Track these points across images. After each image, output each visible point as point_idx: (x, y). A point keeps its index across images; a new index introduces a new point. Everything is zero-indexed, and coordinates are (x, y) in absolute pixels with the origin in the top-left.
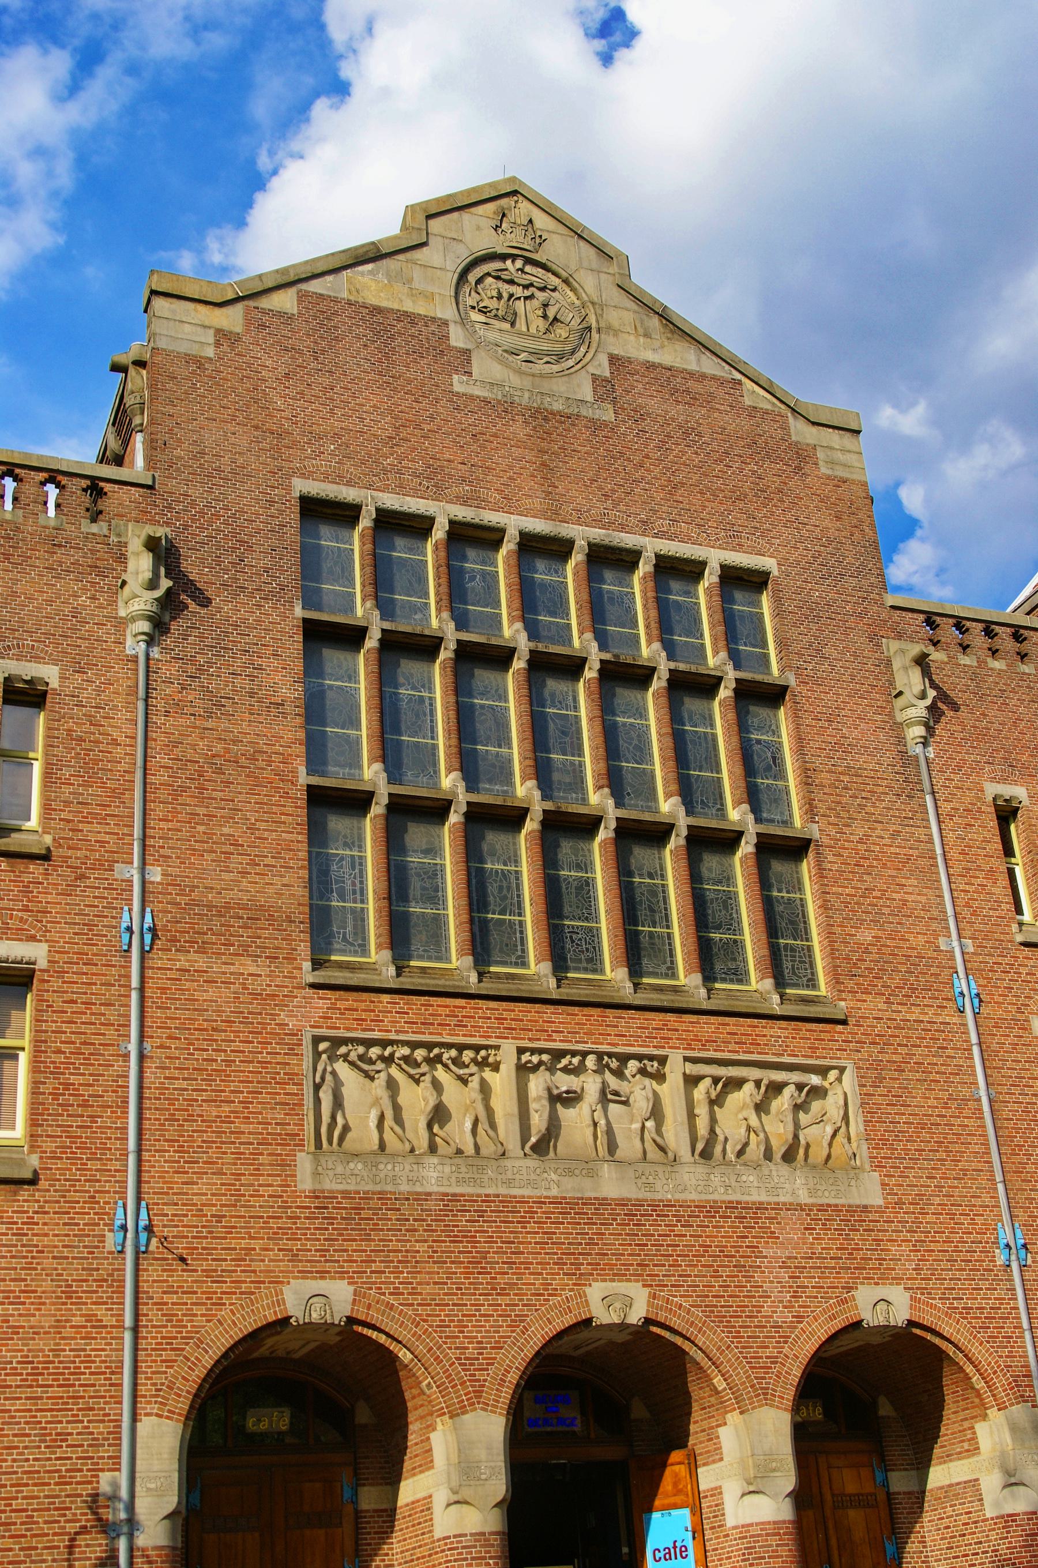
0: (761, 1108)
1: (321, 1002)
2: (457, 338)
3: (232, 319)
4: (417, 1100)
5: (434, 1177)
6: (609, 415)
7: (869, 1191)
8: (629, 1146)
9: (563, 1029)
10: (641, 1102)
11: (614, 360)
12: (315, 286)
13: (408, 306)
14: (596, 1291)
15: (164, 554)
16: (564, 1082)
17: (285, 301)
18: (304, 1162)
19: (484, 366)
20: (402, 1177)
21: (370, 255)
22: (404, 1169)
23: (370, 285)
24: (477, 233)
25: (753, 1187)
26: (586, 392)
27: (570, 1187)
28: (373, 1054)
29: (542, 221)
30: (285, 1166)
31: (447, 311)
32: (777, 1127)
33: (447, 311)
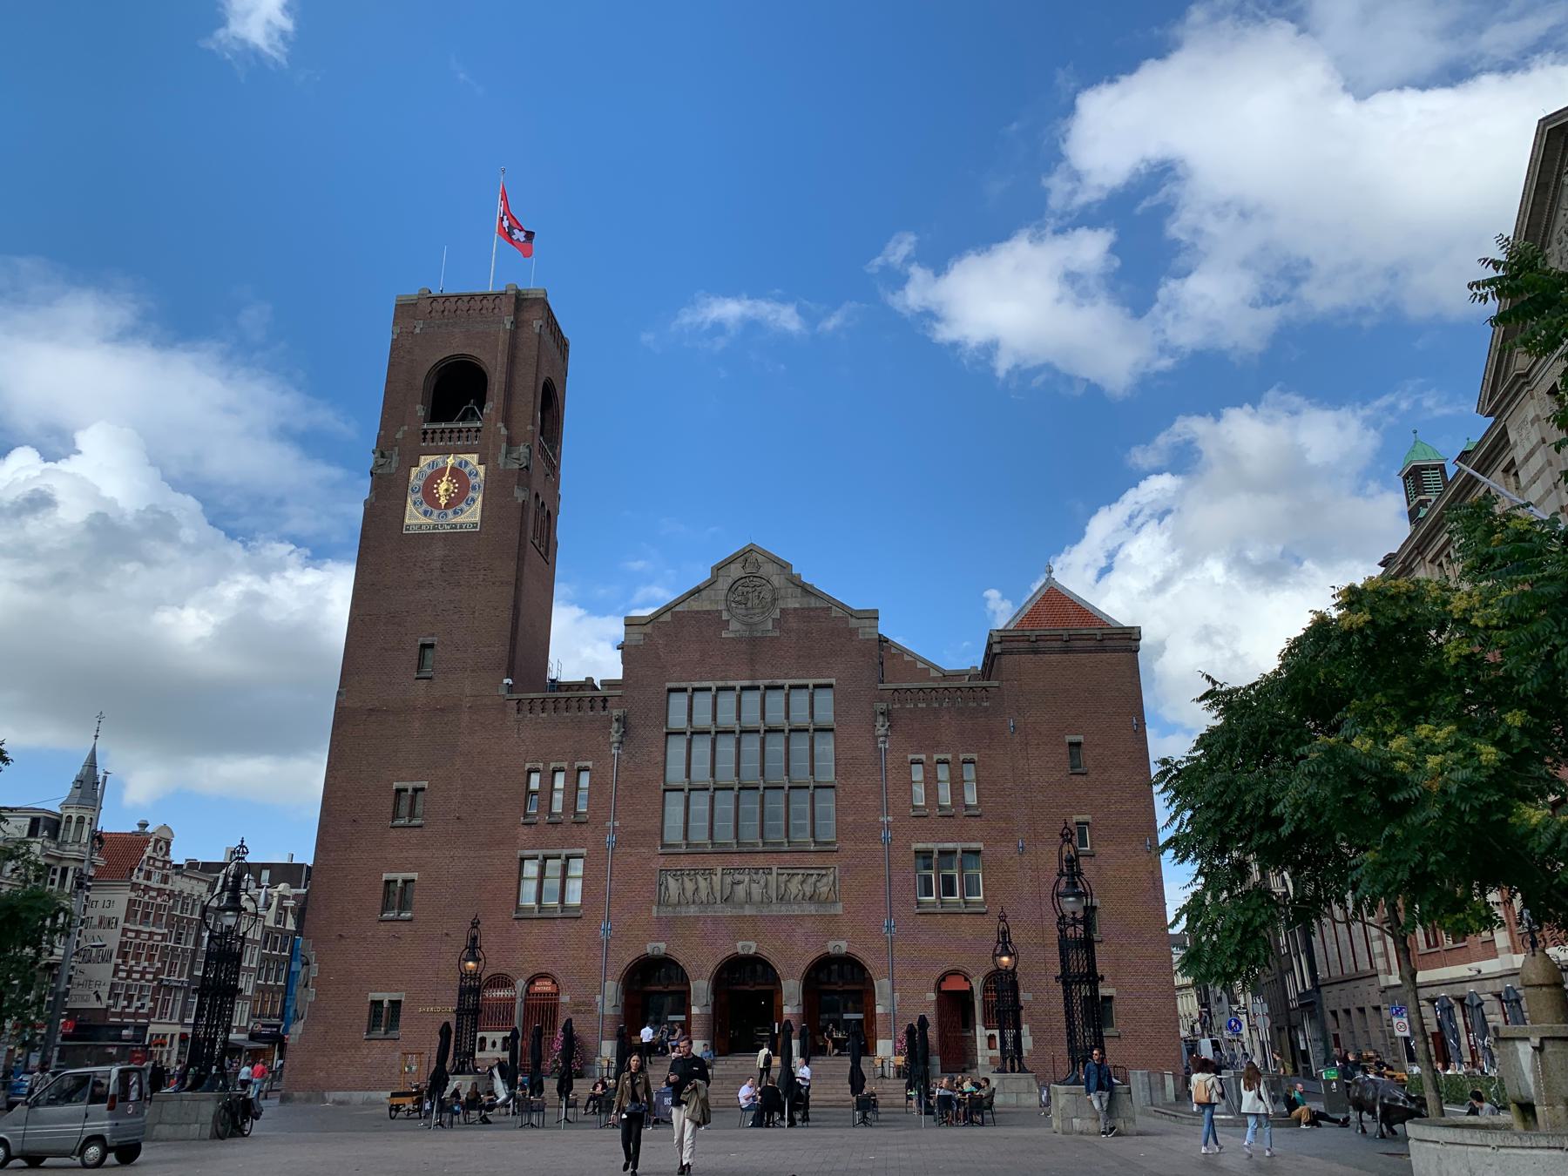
0: (803, 882)
1: (662, 859)
2: (725, 616)
3: (648, 629)
4: (689, 886)
5: (693, 910)
6: (777, 634)
7: (839, 909)
8: (756, 896)
9: (737, 861)
10: (762, 883)
11: (783, 611)
12: (677, 609)
13: (708, 608)
14: (740, 944)
15: (623, 721)
16: (738, 877)
17: (667, 617)
18: (655, 908)
19: (734, 625)
20: (684, 911)
21: (697, 591)
22: (684, 909)
23: (694, 605)
24: (736, 571)
25: (796, 910)
26: (770, 626)
27: (735, 912)
28: (678, 874)
29: (761, 559)
30: (650, 910)
31: (722, 607)
32: (808, 889)
33: (722, 607)
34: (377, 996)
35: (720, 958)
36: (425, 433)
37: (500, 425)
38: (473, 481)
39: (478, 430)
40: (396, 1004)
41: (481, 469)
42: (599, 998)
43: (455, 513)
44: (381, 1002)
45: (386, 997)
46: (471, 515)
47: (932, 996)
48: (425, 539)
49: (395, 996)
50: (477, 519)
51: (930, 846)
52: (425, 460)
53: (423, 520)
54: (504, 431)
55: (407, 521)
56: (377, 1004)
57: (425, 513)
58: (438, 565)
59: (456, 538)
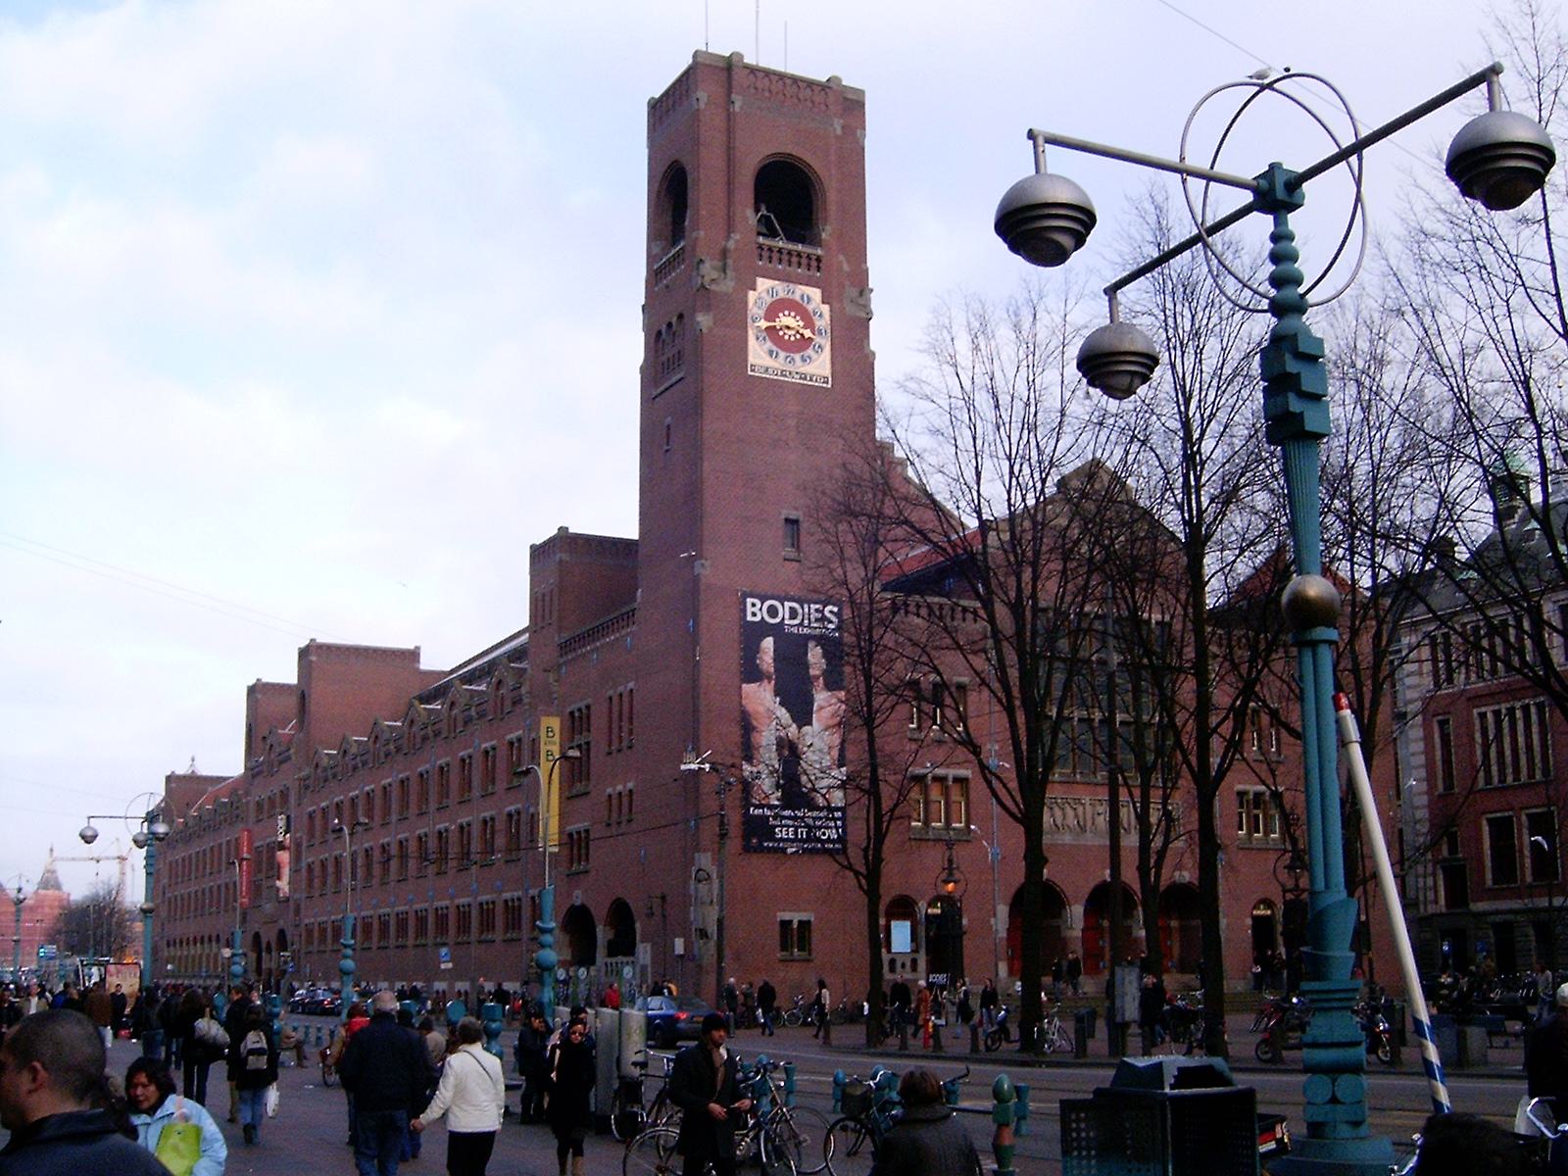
34: (786, 916)
35: (1092, 884)
36: (761, 247)
37: (841, 258)
38: (820, 323)
39: (819, 259)
40: (805, 925)
41: (826, 309)
42: (993, 921)
43: (804, 360)
44: (791, 921)
45: (796, 917)
46: (819, 365)
47: (1249, 921)
48: (774, 387)
49: (804, 916)
50: (827, 372)
51: (1248, 787)
52: (763, 284)
53: (769, 362)
54: (846, 267)
55: (751, 360)
56: (785, 925)
57: (771, 353)
58: (792, 422)
59: (806, 392)
